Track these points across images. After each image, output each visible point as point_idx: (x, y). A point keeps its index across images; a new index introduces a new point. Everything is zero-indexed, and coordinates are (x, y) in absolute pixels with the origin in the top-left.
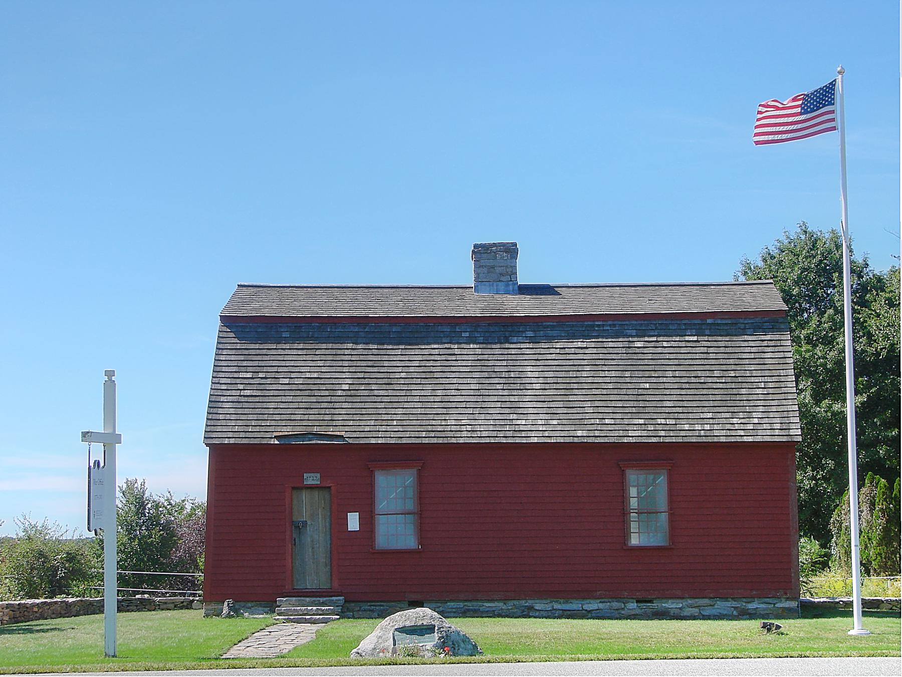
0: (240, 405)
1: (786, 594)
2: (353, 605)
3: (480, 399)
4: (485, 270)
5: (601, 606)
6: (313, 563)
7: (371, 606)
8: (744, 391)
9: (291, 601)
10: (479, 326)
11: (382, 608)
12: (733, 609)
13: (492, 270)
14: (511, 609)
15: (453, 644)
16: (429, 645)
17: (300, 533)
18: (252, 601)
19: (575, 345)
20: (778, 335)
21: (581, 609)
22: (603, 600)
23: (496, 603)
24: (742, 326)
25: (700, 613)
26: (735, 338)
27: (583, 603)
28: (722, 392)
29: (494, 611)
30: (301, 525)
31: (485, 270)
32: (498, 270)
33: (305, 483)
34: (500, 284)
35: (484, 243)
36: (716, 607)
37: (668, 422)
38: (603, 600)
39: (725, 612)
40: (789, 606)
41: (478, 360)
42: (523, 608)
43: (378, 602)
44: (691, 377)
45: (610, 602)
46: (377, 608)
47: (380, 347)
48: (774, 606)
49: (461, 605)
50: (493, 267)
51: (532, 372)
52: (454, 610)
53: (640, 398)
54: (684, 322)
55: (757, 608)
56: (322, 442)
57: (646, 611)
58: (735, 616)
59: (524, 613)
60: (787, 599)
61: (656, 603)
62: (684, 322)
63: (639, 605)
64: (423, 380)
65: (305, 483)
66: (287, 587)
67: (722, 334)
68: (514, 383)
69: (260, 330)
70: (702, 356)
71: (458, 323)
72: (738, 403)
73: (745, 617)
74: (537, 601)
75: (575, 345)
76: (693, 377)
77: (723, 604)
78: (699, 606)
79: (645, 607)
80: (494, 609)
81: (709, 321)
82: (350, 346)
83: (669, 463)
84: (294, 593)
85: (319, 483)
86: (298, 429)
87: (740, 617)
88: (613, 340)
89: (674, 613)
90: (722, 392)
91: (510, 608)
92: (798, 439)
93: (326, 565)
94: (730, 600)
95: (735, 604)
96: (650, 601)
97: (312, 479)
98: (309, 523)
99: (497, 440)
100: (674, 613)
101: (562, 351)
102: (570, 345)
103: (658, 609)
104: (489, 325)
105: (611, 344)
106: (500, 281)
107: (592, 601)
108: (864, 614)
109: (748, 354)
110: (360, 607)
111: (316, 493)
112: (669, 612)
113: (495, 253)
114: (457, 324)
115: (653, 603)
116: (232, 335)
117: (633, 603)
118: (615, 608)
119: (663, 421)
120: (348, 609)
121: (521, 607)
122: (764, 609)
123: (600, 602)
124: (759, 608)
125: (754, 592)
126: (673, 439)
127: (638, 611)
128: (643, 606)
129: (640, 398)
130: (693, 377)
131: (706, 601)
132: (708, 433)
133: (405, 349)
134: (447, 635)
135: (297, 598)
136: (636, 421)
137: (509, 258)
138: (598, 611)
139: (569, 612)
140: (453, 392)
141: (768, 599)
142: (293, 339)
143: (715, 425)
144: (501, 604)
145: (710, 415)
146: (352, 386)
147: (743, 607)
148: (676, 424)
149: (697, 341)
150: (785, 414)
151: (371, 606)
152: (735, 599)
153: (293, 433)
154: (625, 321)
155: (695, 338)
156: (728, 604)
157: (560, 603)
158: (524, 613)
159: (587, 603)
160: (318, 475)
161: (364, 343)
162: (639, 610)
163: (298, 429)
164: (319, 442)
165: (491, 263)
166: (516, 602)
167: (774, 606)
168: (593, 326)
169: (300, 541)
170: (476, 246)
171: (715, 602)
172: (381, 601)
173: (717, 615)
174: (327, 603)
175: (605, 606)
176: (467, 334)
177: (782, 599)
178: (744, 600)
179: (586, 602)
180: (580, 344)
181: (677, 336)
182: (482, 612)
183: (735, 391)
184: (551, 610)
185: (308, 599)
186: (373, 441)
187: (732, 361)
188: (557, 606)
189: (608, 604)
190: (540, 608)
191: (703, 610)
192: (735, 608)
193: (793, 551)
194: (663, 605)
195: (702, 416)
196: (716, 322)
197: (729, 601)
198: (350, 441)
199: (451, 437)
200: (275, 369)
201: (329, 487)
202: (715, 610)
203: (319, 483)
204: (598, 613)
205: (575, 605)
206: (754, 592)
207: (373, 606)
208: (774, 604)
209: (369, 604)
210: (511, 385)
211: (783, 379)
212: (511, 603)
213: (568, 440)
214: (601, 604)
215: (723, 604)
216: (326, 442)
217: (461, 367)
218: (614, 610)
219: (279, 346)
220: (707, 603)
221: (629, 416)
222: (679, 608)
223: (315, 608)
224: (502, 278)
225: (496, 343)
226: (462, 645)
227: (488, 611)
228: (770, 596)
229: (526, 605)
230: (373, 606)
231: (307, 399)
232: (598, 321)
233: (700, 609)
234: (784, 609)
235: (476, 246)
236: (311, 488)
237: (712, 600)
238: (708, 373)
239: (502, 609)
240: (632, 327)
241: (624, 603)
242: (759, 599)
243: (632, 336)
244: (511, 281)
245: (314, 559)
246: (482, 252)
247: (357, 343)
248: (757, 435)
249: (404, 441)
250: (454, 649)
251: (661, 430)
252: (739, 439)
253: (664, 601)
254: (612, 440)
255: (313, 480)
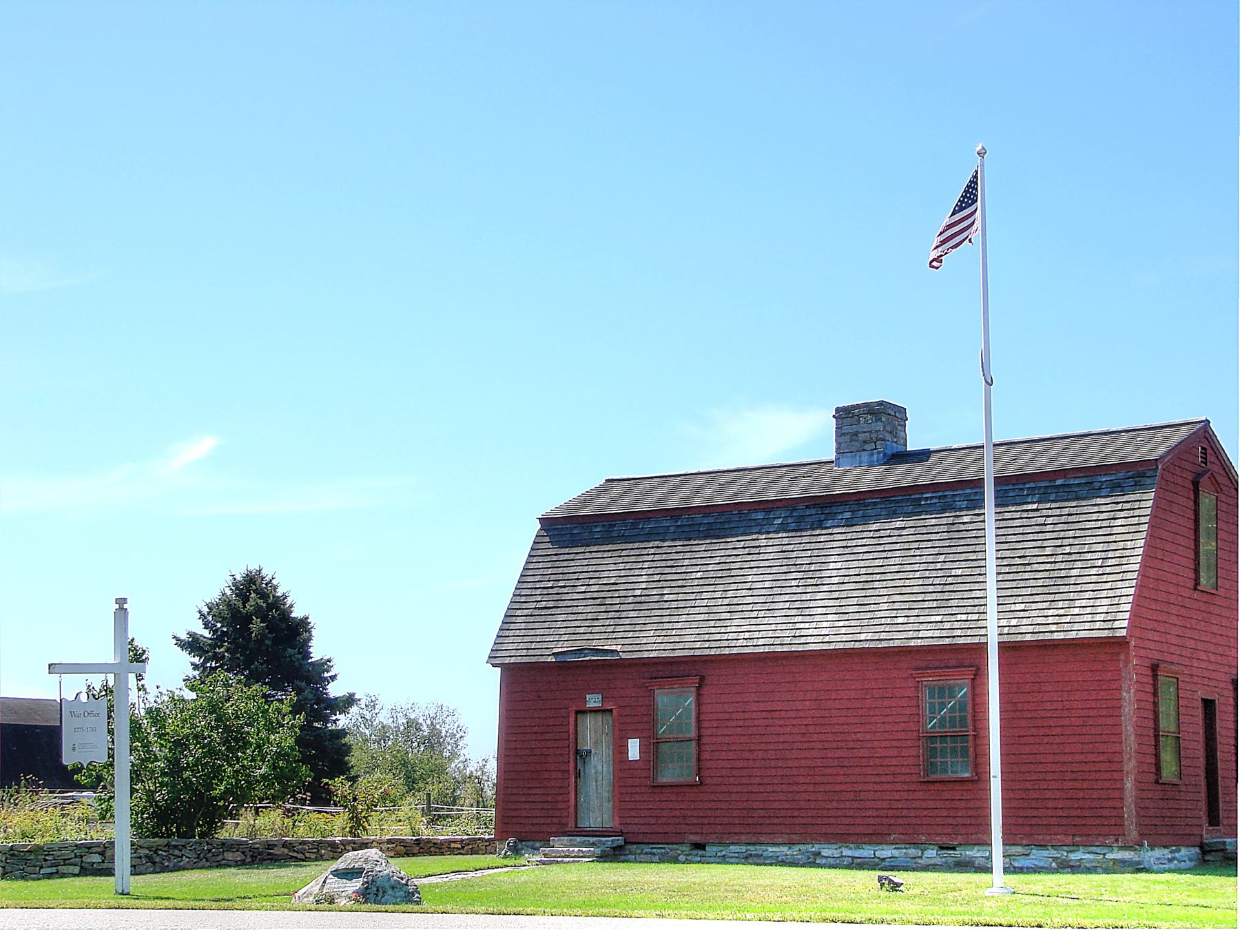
0: (532, 619)
1: (1117, 840)
2: (635, 846)
3: (770, 599)
4: (847, 438)
5: (896, 853)
6: (597, 797)
7: (652, 848)
8: (1074, 573)
9: (563, 840)
10: (796, 509)
11: (663, 850)
12: (1051, 859)
13: (855, 437)
14: (796, 855)
15: (378, 890)
16: (350, 890)
17: (584, 762)
18: (541, 841)
19: (893, 525)
20: (1139, 495)
21: (873, 856)
22: (899, 846)
23: (781, 847)
24: (1097, 485)
25: (1011, 863)
26: (1084, 503)
27: (876, 849)
28: (1046, 574)
29: (778, 857)
30: (584, 754)
31: (847, 438)
32: (862, 437)
33: (587, 706)
34: (863, 453)
35: (846, 405)
36: (1031, 856)
37: (970, 617)
38: (899, 846)
39: (1041, 864)
40: (1121, 857)
41: (782, 552)
42: (809, 854)
43: (659, 843)
44: (1015, 557)
45: (906, 849)
46: (658, 851)
47: (685, 543)
48: (1104, 857)
49: (744, 849)
50: (856, 434)
51: (836, 562)
52: (736, 855)
53: (947, 588)
54: (1027, 486)
55: (1081, 859)
56: (596, 658)
57: (947, 860)
58: (1055, 869)
59: (809, 860)
60: (1121, 848)
61: (960, 850)
62: (1027, 486)
63: (939, 853)
64: (717, 579)
65: (587, 706)
66: (570, 825)
67: (1070, 497)
68: (812, 578)
69: (575, 532)
70: (1037, 529)
71: (773, 508)
72: (1063, 589)
73: (1066, 871)
74: (826, 846)
75: (893, 525)
76: (1018, 557)
77: (1039, 853)
78: (1009, 855)
79: (945, 855)
80: (779, 854)
81: (1059, 482)
82: (657, 543)
83: (970, 671)
84: (577, 832)
85: (601, 705)
86: (578, 643)
87: (1060, 870)
88: (937, 516)
89: (979, 864)
90: (1046, 574)
91: (795, 853)
92: (1121, 632)
93: (609, 801)
94: (1050, 848)
95: (1053, 853)
96: (954, 849)
97: (594, 701)
98: (593, 751)
99: (772, 649)
100: (979, 864)
101: (877, 534)
102: (887, 526)
103: (961, 859)
104: (807, 507)
105: (933, 522)
106: (864, 450)
107: (885, 847)
108: (1006, 870)
109: (1094, 523)
110: (642, 850)
111: (600, 717)
112: (973, 863)
113: (858, 416)
114: (772, 510)
115: (956, 850)
116: (547, 539)
117: (932, 849)
118: (911, 856)
119: (964, 617)
120: (630, 851)
121: (807, 852)
122: (1091, 861)
123: (895, 848)
124: (1084, 859)
125: (1078, 839)
126: (968, 640)
127: (938, 861)
128: (943, 854)
129: (947, 588)
130: (1018, 557)
131: (1019, 849)
132: (1013, 630)
133: (711, 543)
134: (373, 881)
135: (569, 838)
136: (933, 619)
137: (874, 420)
138: (893, 859)
139: (859, 860)
140: (744, 593)
141: (1095, 848)
142: (608, 539)
143: (1024, 619)
144: (785, 849)
145: (1022, 607)
146: (645, 591)
147: (1064, 857)
148: (978, 620)
149: (1037, 510)
150: (1116, 601)
151: (652, 848)
152: (1055, 847)
153: (572, 649)
154: (957, 490)
155: (1035, 506)
156: (1045, 853)
157: (851, 849)
158: (809, 860)
159: (879, 849)
160: (600, 696)
161: (660, 540)
162: (939, 859)
163: (578, 643)
164: (593, 658)
165: (854, 428)
166: (801, 847)
167: (1104, 857)
168: (920, 499)
169: (584, 770)
170: (837, 410)
171: (1029, 851)
172: (663, 843)
173: (1032, 868)
174: (596, 843)
175: (900, 853)
176: (780, 521)
177: (1114, 848)
178: (1065, 848)
179: (879, 848)
180: (898, 524)
181: (1013, 505)
182: (766, 858)
183: (1063, 573)
184: (839, 857)
185: (578, 839)
186: (646, 655)
187: (1071, 534)
188: (847, 852)
189: (904, 851)
190: (827, 855)
191: (1014, 860)
192: (1055, 859)
193: (1126, 784)
194: (967, 853)
195: (1013, 607)
196: (1067, 483)
197: (1048, 849)
198: (623, 656)
199: (725, 647)
200: (576, 576)
201: (611, 711)
202: (1029, 861)
203: (601, 705)
204: (891, 862)
205: (866, 852)
206: (1078, 839)
207: (655, 848)
208: (1104, 854)
209: (651, 846)
210: (808, 580)
211: (1127, 553)
212: (797, 848)
213: (848, 645)
214: (896, 850)
215: (1039, 853)
216: (599, 658)
217: (761, 562)
218: (910, 858)
219: (588, 549)
220: (1019, 852)
221: (926, 612)
222: (985, 857)
223: (576, 849)
224: (867, 447)
225: (806, 530)
226: (390, 892)
227: (771, 857)
228: (1096, 844)
229: (812, 850)
230: (655, 848)
231: (596, 609)
232: (926, 493)
233: (1010, 860)
234: (1115, 860)
235: (837, 410)
236: (595, 711)
237: (1027, 848)
238: (1036, 552)
239: (786, 855)
240: (912, 502)
241: (922, 850)
242: (1085, 848)
243: (961, 509)
244: (876, 449)
245: (597, 793)
246: (843, 416)
247: (663, 541)
248: (1072, 630)
249: (677, 653)
250: (377, 896)
251: (957, 629)
252: (1048, 637)
253: (969, 847)
254: (897, 643)
255: (595, 702)
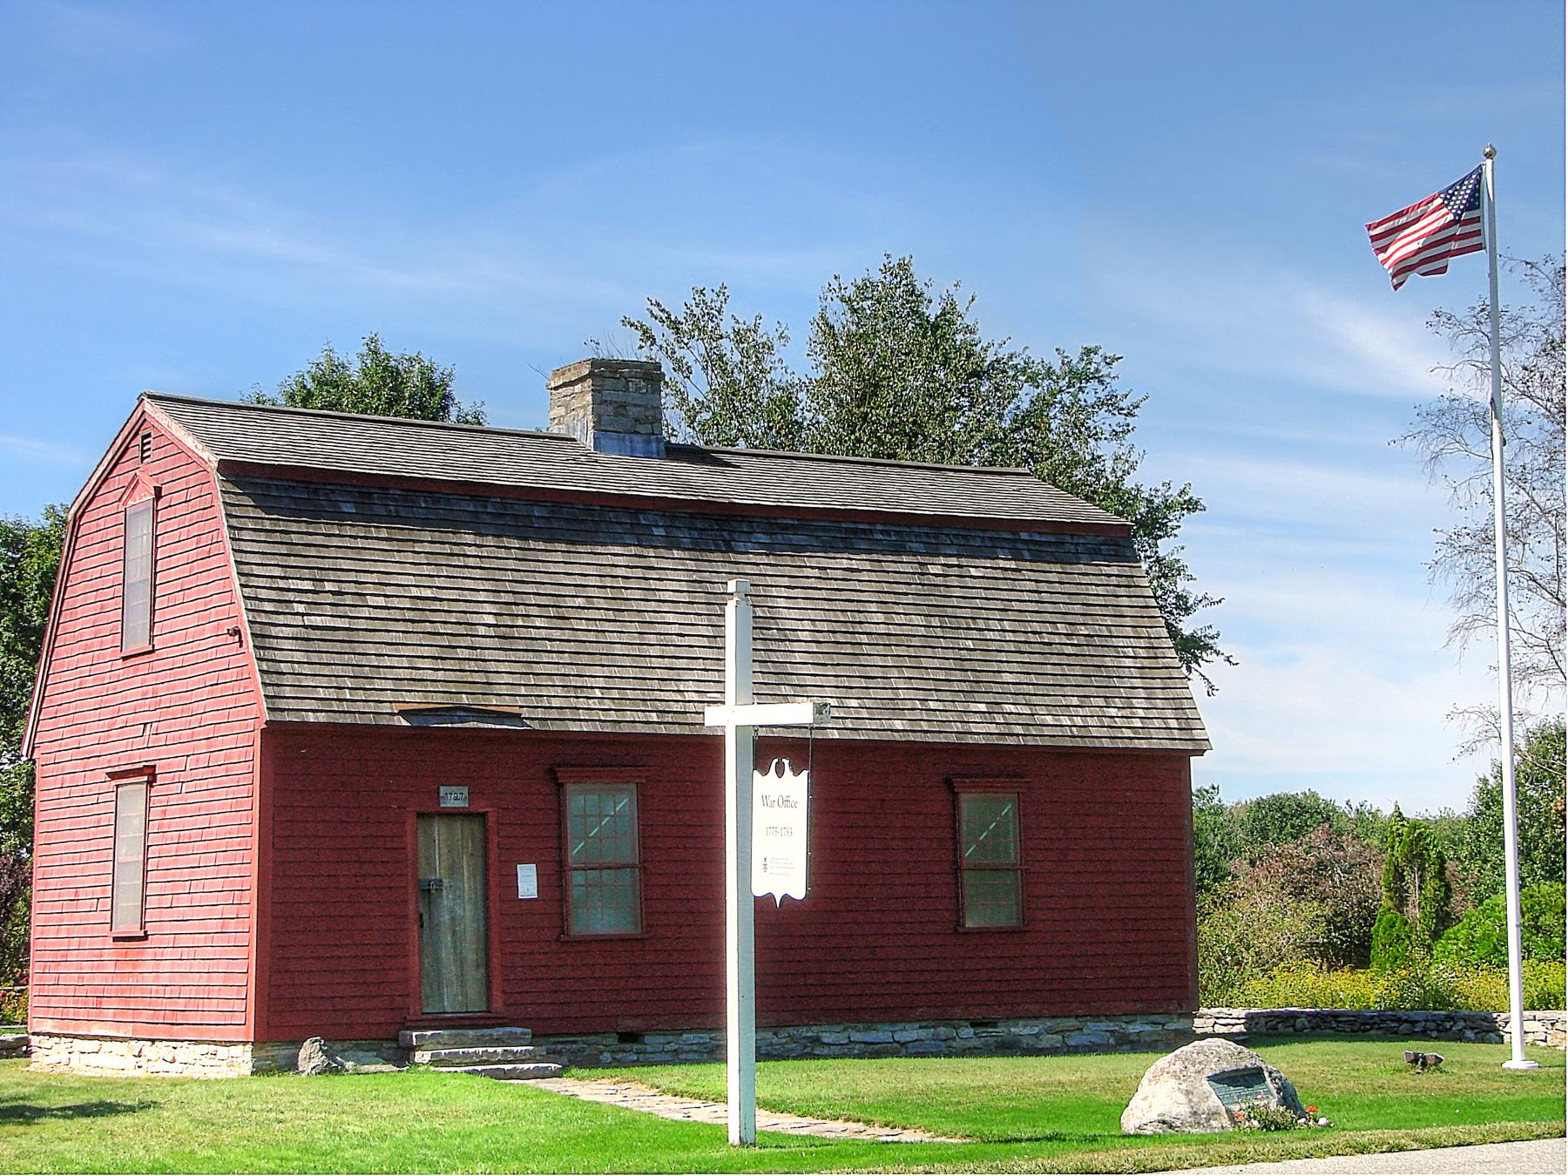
5: (922, 1033)
12: (1108, 1034)
13: (621, 410)
14: (785, 1043)
17: (430, 902)
22: (925, 1024)
32: (632, 411)
33: (442, 805)
34: (636, 438)
38: (925, 1024)
45: (933, 1027)
48: (1163, 1029)
50: (623, 406)
52: (695, 1048)
54: (989, 534)
74: (826, 1028)
86: (439, 698)
93: (478, 966)
94: (1104, 1018)
95: (1112, 1026)
96: (994, 1025)
97: (454, 797)
98: (446, 882)
106: (636, 433)
111: (458, 825)
122: (1151, 1034)
123: (920, 1027)
127: (975, 1042)
131: (1072, 1022)
137: (650, 391)
138: (917, 1043)
142: (367, 516)
152: (1111, 1018)
156: (1103, 1026)
160: (465, 790)
165: (619, 396)
172: (573, 1035)
184: (847, 1044)
185: (471, 1033)
188: (856, 1036)
192: (1112, 1032)
194: (1012, 1030)
197: (1101, 1021)
201: (484, 815)
205: (881, 1034)
207: (559, 1043)
208: (1163, 1025)
209: (552, 1040)
212: (784, 1033)
216: (493, 726)
223: (499, 1050)
224: (640, 428)
239: (771, 1044)
244: (653, 434)
246: (607, 374)
249: (626, 729)
255: (456, 799)
